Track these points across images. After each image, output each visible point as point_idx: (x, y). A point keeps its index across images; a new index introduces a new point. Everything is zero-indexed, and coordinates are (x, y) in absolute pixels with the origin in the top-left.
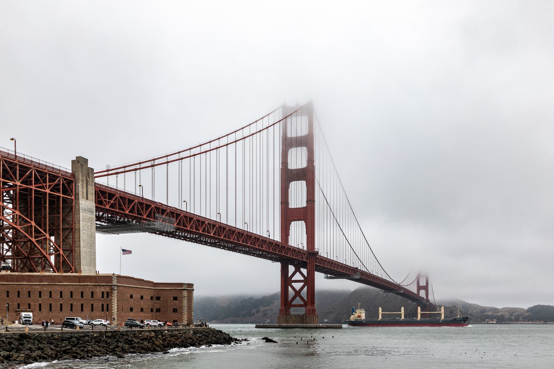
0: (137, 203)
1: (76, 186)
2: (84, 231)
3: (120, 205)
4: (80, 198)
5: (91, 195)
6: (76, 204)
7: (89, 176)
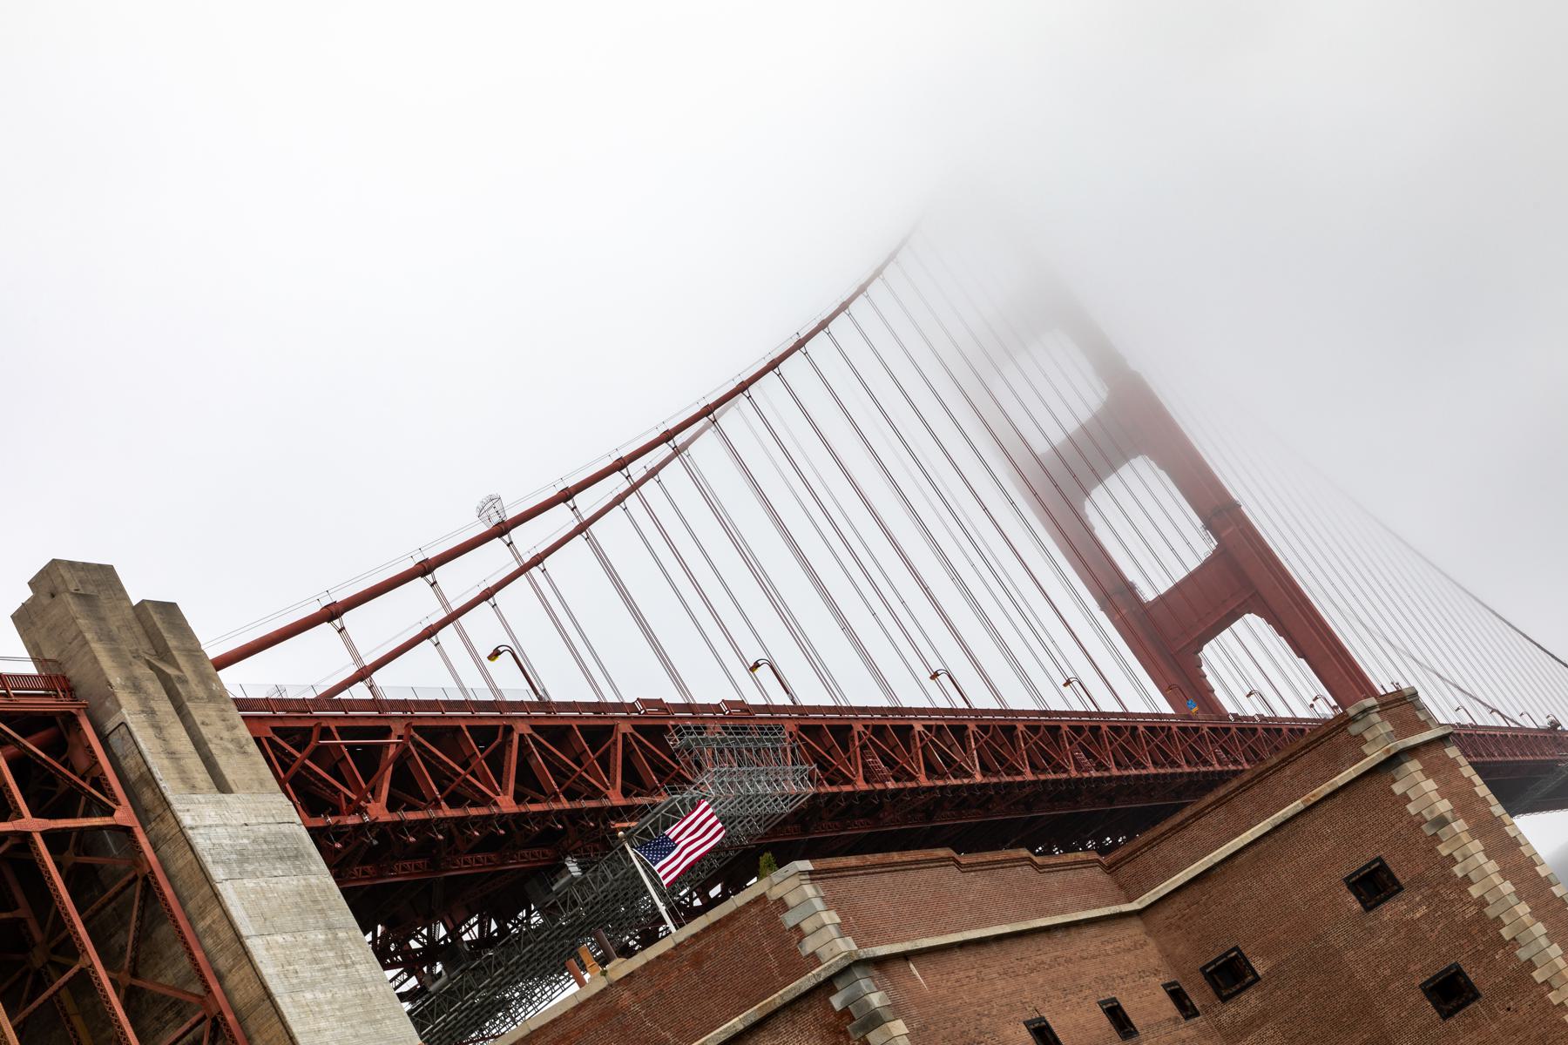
0: (530, 735)
1: (113, 739)
2: (309, 996)
3: (442, 776)
4: (171, 796)
5: (237, 757)
6: (164, 848)
7: (164, 653)
